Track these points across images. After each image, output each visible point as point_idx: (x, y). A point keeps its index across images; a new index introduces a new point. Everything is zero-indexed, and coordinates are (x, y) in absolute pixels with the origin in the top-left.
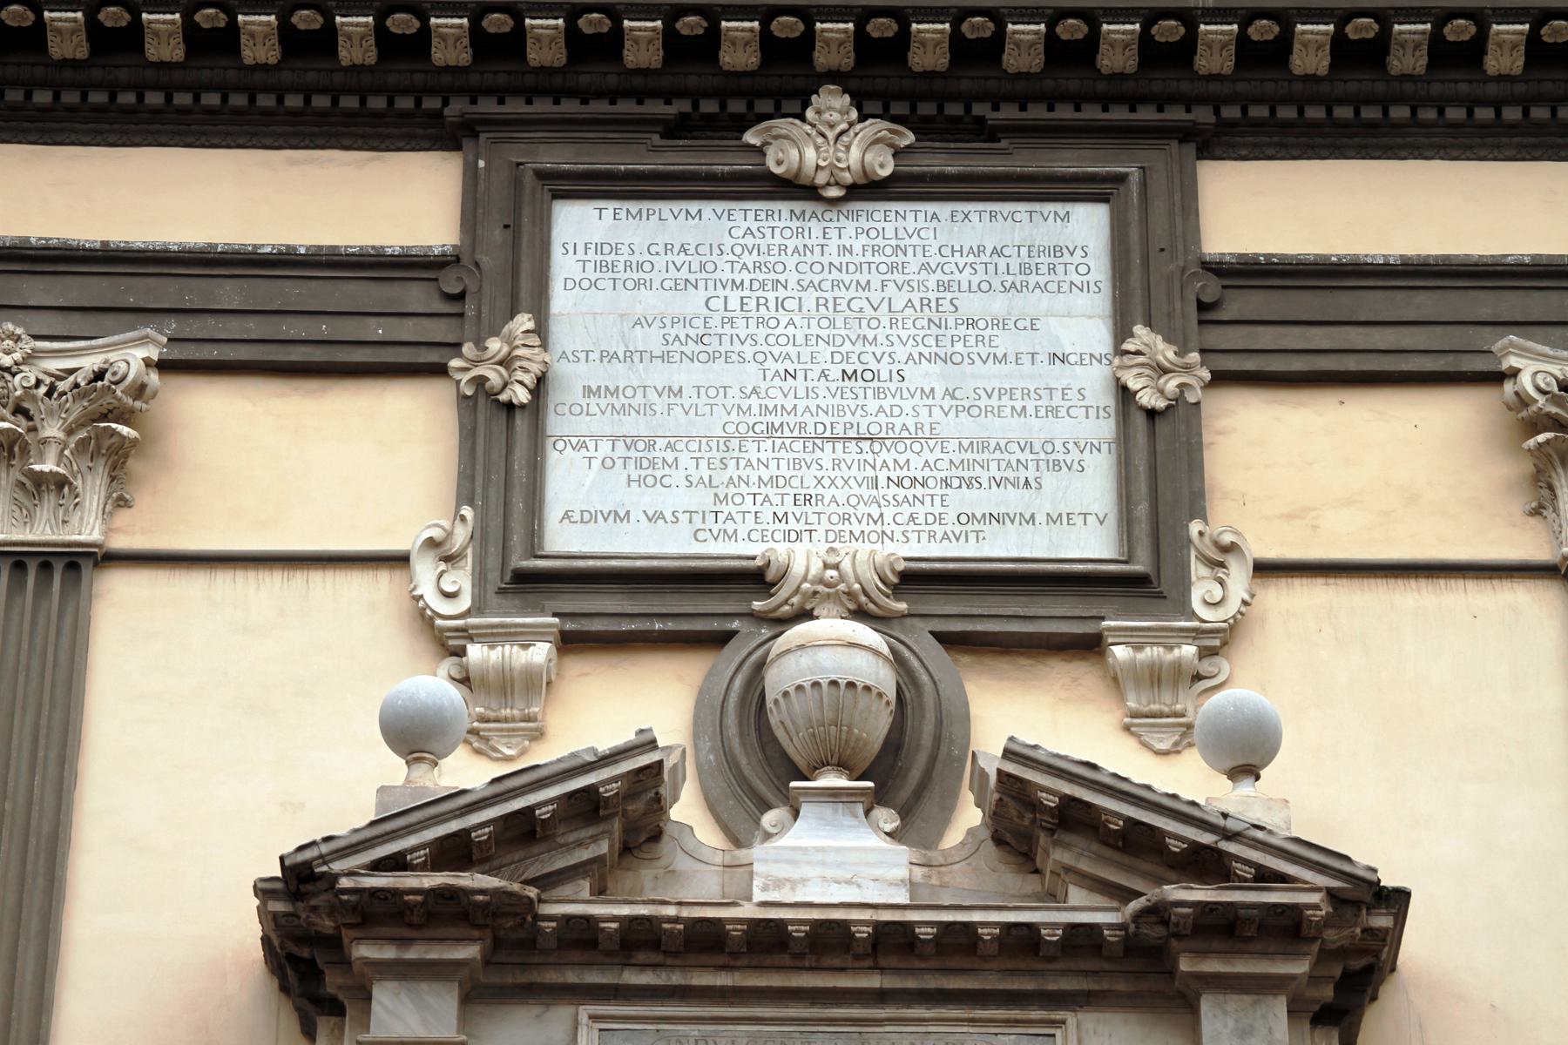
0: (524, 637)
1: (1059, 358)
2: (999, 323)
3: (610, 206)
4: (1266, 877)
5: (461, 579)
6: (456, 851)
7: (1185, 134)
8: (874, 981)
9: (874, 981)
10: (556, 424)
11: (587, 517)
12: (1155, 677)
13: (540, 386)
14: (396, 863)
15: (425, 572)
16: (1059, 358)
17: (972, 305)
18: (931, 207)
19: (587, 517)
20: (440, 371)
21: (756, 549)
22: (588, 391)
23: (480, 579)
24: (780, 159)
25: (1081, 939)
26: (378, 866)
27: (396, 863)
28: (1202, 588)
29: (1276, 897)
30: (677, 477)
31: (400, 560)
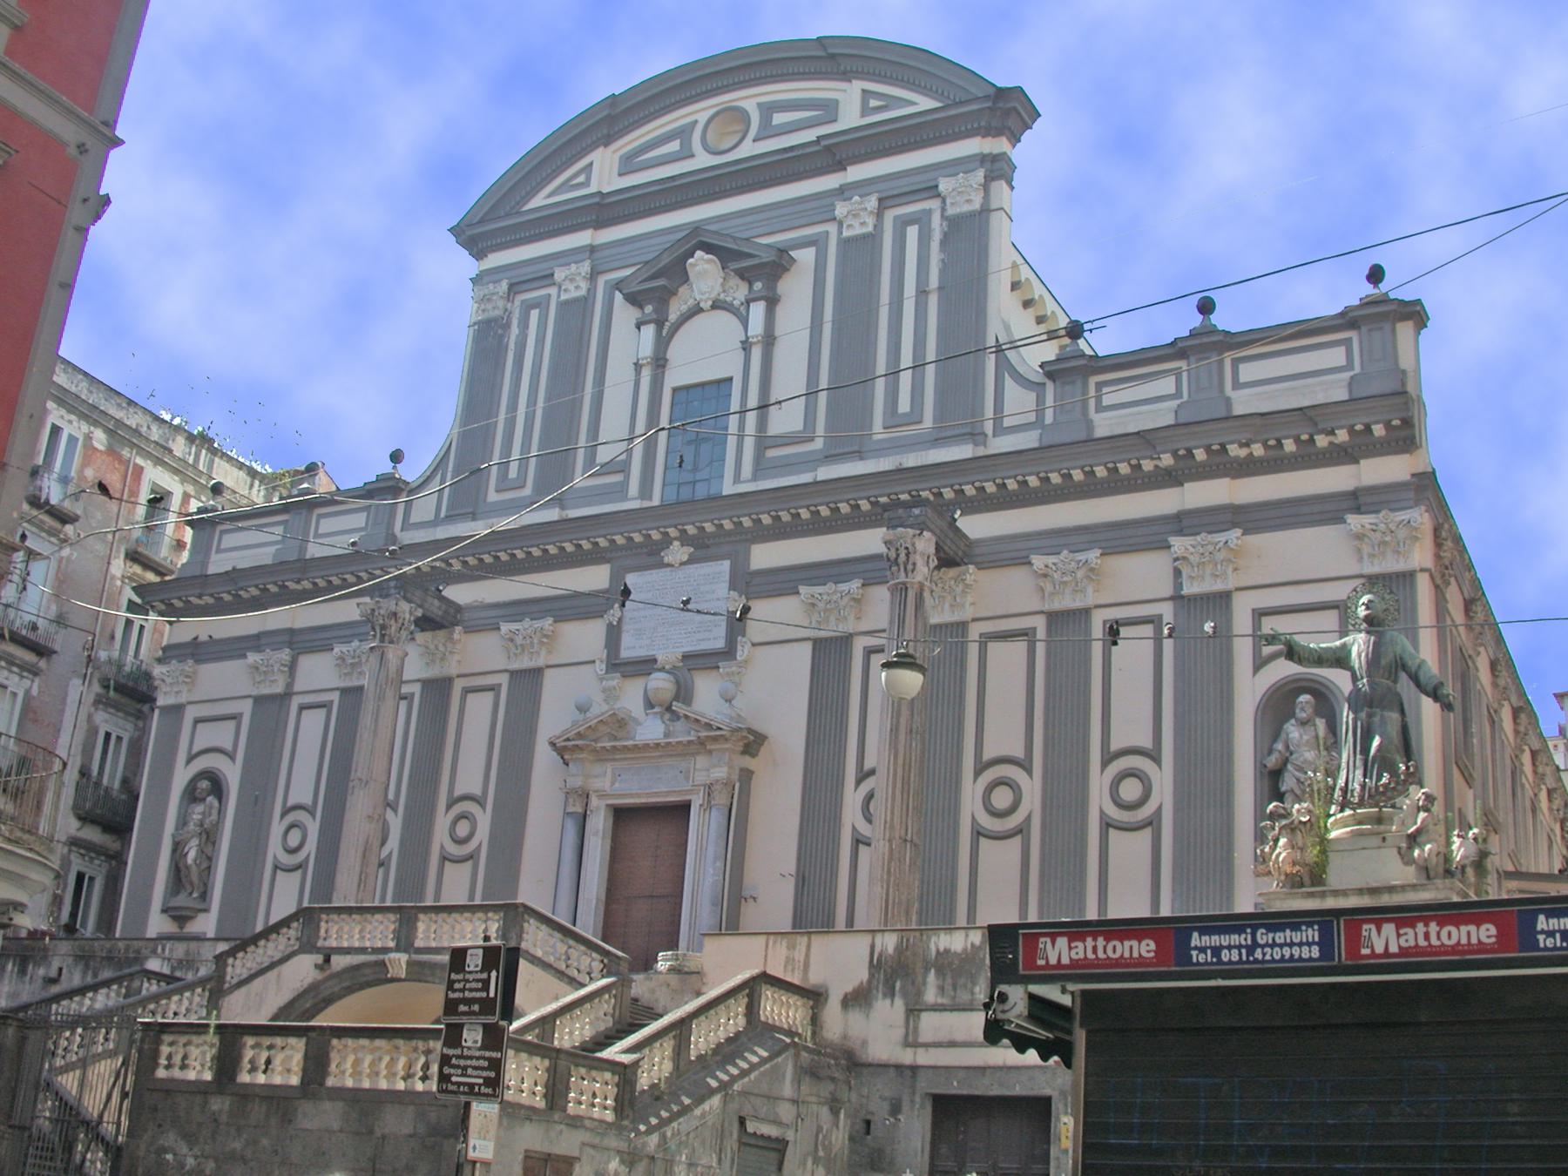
0: (613, 679)
1: (718, 599)
2: (707, 592)
3: (636, 573)
4: (719, 729)
5: (604, 666)
6: (580, 736)
7: (747, 540)
8: (658, 754)
9: (658, 754)
10: (625, 627)
11: (628, 648)
12: (728, 674)
13: (620, 620)
14: (565, 740)
15: (598, 662)
16: (718, 599)
17: (702, 588)
18: (695, 566)
19: (628, 648)
20: (602, 616)
21: (650, 653)
22: (631, 619)
23: (607, 667)
24: (666, 560)
25: (690, 742)
26: (565, 740)
27: (568, 740)
28: (739, 653)
29: (718, 733)
30: (645, 637)
31: (594, 662)
